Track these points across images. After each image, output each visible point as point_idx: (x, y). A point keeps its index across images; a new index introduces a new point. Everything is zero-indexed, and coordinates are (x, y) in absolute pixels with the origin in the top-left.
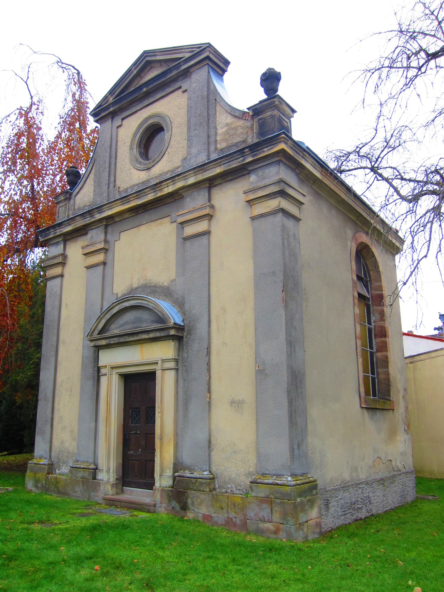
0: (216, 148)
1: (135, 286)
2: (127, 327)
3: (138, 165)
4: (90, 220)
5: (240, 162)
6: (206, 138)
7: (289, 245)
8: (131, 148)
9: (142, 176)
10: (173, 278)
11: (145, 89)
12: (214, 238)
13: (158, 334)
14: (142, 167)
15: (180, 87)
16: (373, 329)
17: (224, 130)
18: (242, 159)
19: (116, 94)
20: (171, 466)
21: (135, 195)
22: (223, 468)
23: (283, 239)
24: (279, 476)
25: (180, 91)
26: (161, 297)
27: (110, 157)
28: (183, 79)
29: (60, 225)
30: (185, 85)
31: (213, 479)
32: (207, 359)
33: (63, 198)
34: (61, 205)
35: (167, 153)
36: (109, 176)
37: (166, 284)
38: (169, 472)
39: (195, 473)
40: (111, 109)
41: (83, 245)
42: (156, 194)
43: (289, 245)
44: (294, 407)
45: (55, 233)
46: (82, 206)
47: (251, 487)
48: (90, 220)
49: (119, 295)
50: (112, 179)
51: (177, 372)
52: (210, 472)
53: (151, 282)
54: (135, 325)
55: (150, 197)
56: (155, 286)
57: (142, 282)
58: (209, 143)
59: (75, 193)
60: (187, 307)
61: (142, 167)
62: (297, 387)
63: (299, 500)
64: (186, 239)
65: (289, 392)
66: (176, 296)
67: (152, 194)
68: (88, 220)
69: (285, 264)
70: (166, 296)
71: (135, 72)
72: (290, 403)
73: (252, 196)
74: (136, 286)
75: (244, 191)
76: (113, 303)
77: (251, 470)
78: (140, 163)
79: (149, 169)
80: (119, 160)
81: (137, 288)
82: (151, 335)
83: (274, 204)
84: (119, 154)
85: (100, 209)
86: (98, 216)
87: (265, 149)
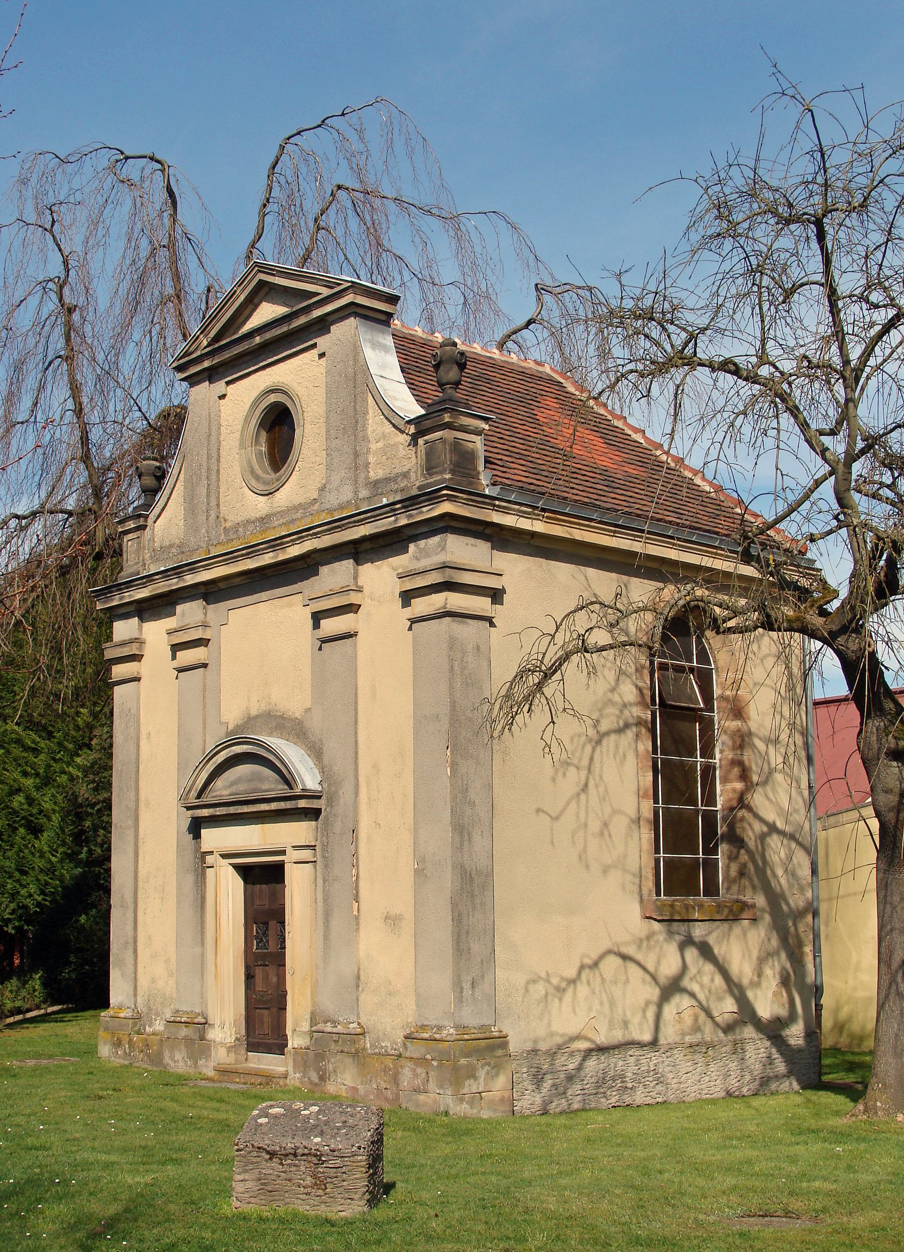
0: (367, 478)
1: (254, 712)
2: (241, 787)
3: (253, 482)
4: (177, 583)
5: (391, 523)
6: (352, 457)
7: (463, 669)
8: (242, 446)
9: (259, 505)
10: (309, 706)
11: (258, 340)
12: (361, 640)
13: (282, 805)
14: (261, 487)
15: (314, 346)
16: (717, 765)
17: (380, 445)
18: (393, 519)
19: (212, 334)
20: (308, 1017)
21: (244, 552)
22: (376, 1019)
23: (451, 660)
24: (440, 1028)
25: (314, 353)
26: (291, 738)
27: (209, 457)
28: (319, 329)
29: (129, 584)
30: (323, 342)
31: (363, 1034)
32: (353, 847)
33: (132, 526)
34: (131, 536)
35: (297, 469)
36: (208, 496)
37: (298, 715)
38: (305, 1026)
39: (339, 1027)
40: (206, 364)
41: (170, 627)
42: (277, 556)
43: (463, 669)
44: (466, 927)
45: (121, 599)
46: (168, 544)
47: (405, 1044)
48: (177, 583)
49: (231, 727)
50: (213, 503)
51: (315, 867)
52: (359, 1024)
53: (277, 708)
54: (253, 785)
55: (267, 559)
56: (282, 717)
57: (264, 707)
58: (356, 468)
59: (152, 517)
60: (326, 760)
61: (261, 487)
62: (472, 896)
63: (463, 1061)
64: (325, 641)
65: (454, 905)
66: (313, 739)
67: (271, 554)
68: (174, 584)
69: (453, 704)
70: (298, 736)
71: (242, 297)
72: (458, 920)
73: (409, 585)
74: (256, 713)
75: (398, 574)
76: (217, 746)
77: (410, 1020)
78: (258, 478)
79: (271, 493)
80: (223, 465)
81: (257, 717)
82: (274, 806)
83: (437, 601)
84: (223, 453)
85: (192, 567)
86: (190, 579)
87: (424, 509)
